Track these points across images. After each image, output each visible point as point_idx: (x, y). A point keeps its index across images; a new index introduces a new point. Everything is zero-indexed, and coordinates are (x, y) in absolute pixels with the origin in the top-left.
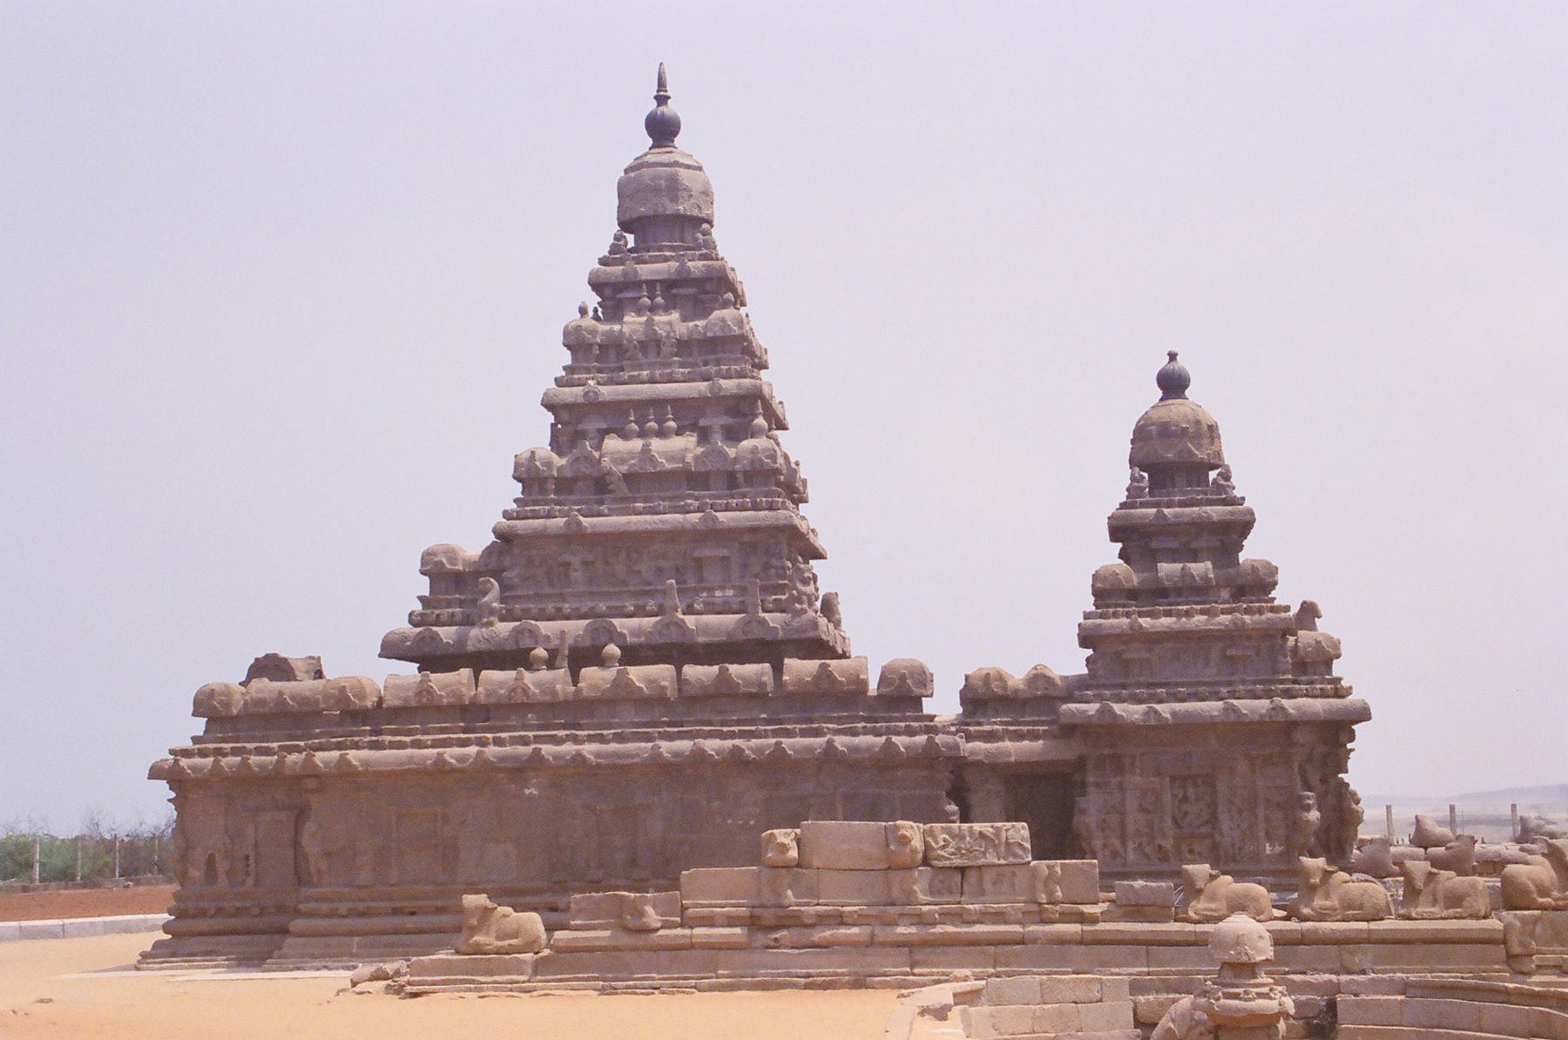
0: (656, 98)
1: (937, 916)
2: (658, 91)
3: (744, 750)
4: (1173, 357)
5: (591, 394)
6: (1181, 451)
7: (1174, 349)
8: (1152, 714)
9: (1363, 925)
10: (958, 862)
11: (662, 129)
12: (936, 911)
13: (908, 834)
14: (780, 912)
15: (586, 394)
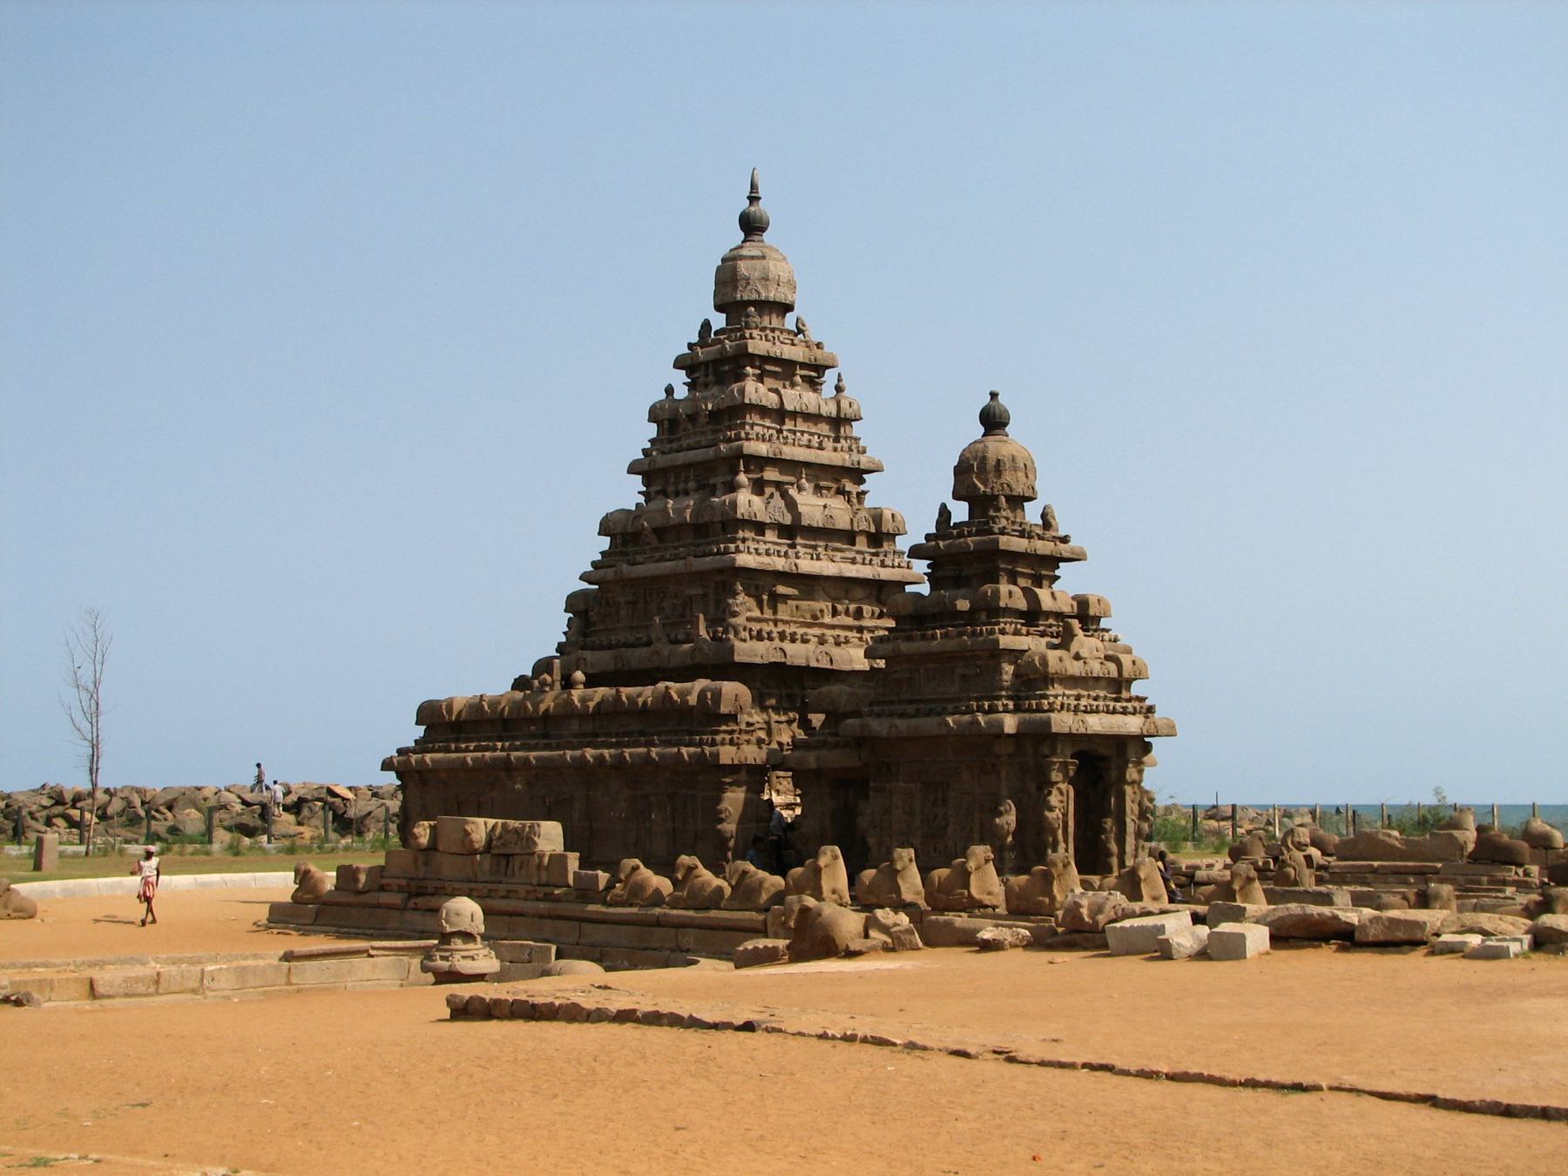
0: (748, 198)
1: (485, 891)
2: (751, 192)
3: (604, 757)
4: (994, 395)
5: (653, 463)
6: (968, 486)
7: (995, 389)
8: (894, 729)
9: (691, 913)
10: (503, 851)
11: (752, 226)
12: (484, 887)
13: (468, 828)
14: (421, 884)
15: (650, 463)
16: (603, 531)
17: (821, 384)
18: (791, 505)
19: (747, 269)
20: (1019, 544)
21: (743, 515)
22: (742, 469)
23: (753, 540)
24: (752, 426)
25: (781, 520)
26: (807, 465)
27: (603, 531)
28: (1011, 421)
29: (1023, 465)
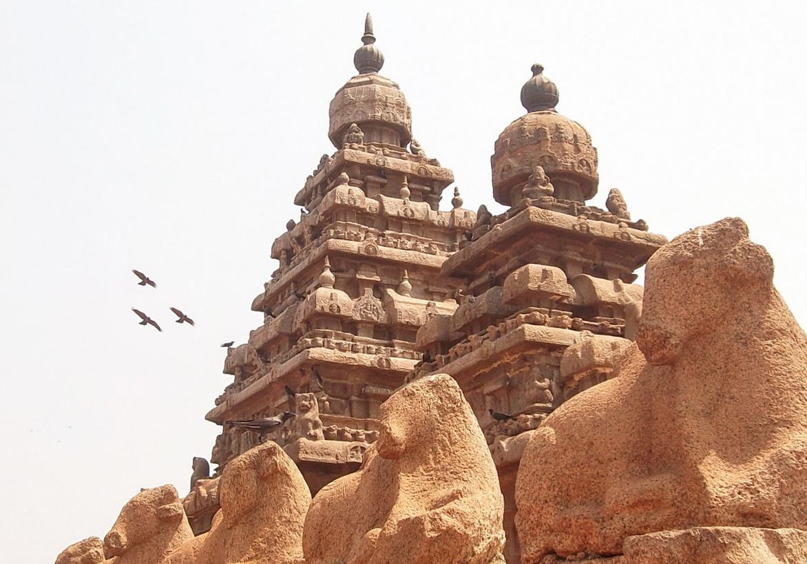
4: (537, 70)
6: (503, 170)
16: (228, 371)
17: (440, 200)
18: (388, 305)
19: (353, 94)
20: (563, 220)
21: (322, 308)
22: (328, 265)
23: (337, 336)
24: (345, 226)
25: (375, 318)
26: (414, 267)
27: (228, 371)
28: (560, 98)
29: (571, 138)
